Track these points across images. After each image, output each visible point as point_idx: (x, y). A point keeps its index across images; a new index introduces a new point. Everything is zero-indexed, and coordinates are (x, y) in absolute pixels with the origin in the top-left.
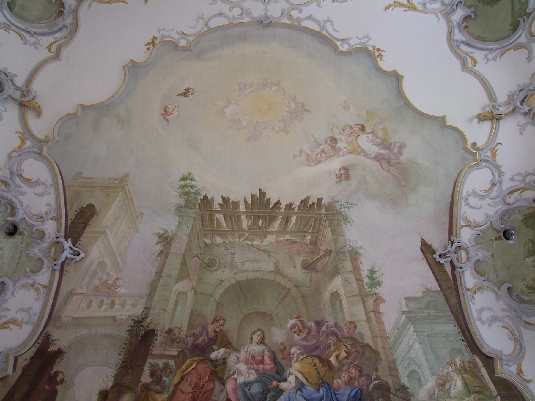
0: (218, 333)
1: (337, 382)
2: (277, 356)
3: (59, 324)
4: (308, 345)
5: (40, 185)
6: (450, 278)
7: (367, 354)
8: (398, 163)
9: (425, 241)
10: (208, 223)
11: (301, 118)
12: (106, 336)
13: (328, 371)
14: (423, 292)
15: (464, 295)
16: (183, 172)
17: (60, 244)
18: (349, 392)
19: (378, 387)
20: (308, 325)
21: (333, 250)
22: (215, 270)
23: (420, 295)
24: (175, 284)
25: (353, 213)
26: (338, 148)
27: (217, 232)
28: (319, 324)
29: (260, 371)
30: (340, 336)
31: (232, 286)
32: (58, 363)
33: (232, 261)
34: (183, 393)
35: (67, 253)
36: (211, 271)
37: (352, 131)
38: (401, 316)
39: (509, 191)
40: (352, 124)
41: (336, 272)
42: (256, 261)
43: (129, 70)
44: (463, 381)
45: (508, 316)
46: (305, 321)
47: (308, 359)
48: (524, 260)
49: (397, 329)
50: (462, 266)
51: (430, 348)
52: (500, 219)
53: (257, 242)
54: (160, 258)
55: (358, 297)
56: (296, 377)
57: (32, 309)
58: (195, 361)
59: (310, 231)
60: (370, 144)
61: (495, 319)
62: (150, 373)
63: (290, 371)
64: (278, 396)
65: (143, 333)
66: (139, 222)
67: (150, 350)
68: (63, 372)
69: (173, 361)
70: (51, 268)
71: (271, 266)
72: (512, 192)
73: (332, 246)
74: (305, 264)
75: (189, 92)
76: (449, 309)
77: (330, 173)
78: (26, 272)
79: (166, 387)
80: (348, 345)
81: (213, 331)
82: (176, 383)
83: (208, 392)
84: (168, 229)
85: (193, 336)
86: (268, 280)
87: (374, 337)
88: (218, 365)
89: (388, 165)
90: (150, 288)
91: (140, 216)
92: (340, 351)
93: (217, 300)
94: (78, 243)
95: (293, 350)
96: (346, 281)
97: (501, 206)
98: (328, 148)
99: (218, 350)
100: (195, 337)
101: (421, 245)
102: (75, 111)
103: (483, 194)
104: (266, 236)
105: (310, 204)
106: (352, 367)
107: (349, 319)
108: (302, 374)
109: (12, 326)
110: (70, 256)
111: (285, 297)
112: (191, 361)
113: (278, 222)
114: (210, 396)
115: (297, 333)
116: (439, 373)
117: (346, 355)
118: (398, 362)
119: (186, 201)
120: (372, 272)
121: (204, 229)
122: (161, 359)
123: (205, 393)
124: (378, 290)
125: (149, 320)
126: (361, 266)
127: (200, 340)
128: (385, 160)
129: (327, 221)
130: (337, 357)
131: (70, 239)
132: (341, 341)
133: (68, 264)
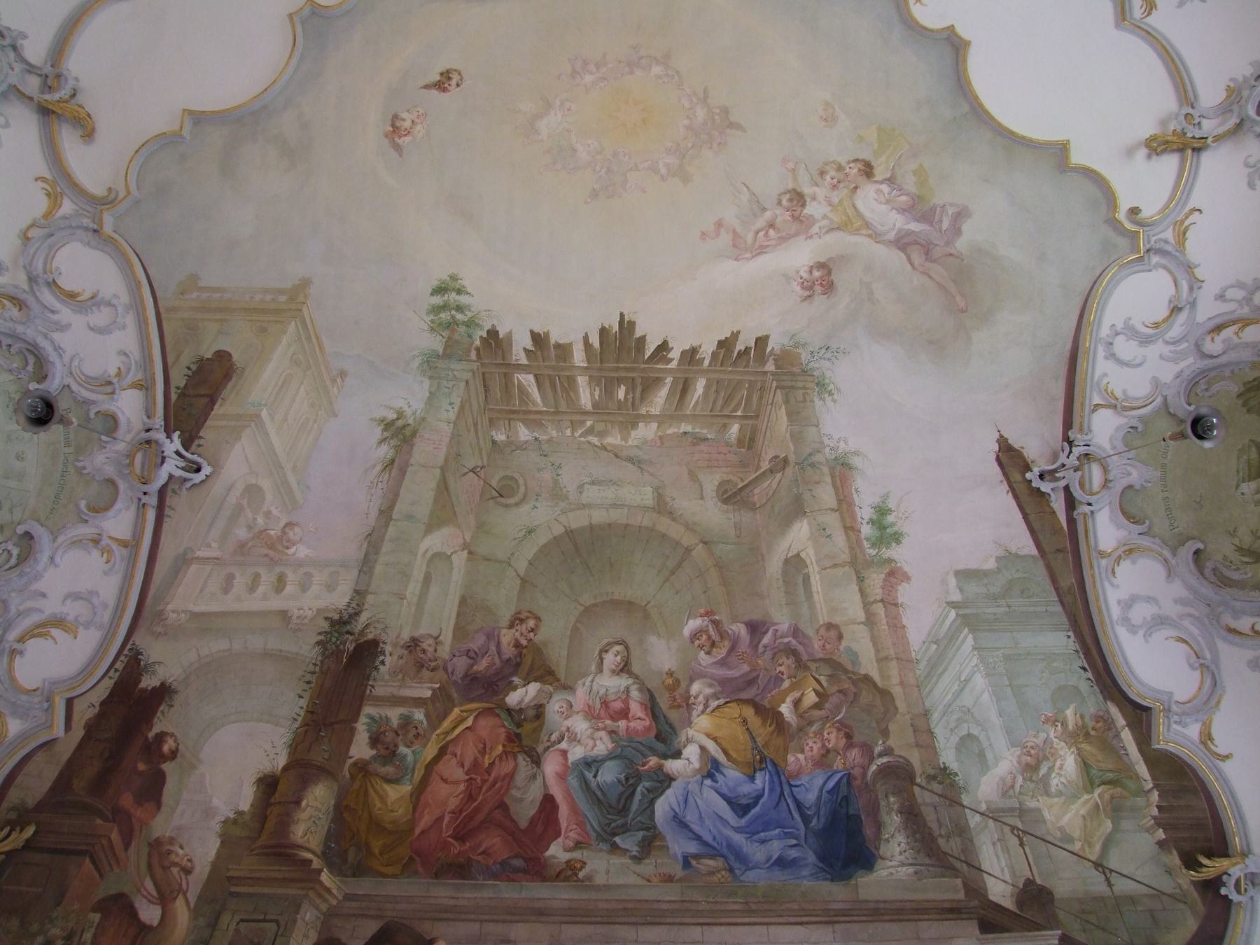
0: (523, 648)
1: (794, 760)
2: (658, 700)
3: (160, 629)
4: (730, 676)
5: (102, 308)
6: (1062, 528)
7: (866, 697)
8: (951, 255)
9: (1007, 439)
10: (499, 395)
11: (720, 143)
12: (266, 655)
13: (776, 734)
14: (998, 559)
15: (1092, 567)
16: (440, 274)
17: (153, 445)
18: (821, 782)
19: (885, 771)
20: (730, 632)
21: (792, 458)
22: (517, 504)
23: (991, 564)
24: (425, 536)
25: (840, 373)
26: (807, 219)
27: (521, 416)
28: (756, 628)
29: (621, 734)
30: (805, 657)
31: (557, 540)
32: (163, 712)
33: (556, 482)
34: (445, 781)
35: (172, 467)
36: (506, 506)
37: (840, 176)
38: (945, 612)
39: (1211, 324)
41: (797, 509)
42: (612, 482)
43: (303, 23)
44: (1080, 759)
45: (1190, 615)
46: (725, 621)
47: (729, 707)
48: (1237, 486)
49: (935, 643)
50: (1092, 499)
51: (1010, 685)
52: (1185, 391)
53: (614, 440)
54: (387, 475)
55: (847, 568)
56: (703, 748)
57: (97, 593)
58: (471, 711)
59: (739, 413)
60: (884, 208)
61: (1160, 621)
62: (370, 738)
63: (687, 734)
64: (661, 790)
65: (351, 648)
66: (336, 392)
67: (369, 687)
68: (176, 734)
69: (422, 710)
70: (136, 501)
71: (647, 496)
72: (1219, 328)
73: (790, 450)
74: (726, 491)
75: (450, 79)
76: (1056, 599)
77: (787, 277)
78: (79, 511)
79: (407, 770)
80: (822, 677)
81: (512, 645)
82: (429, 759)
83: (503, 780)
84: (406, 408)
85: (467, 655)
86: (640, 527)
87: (882, 660)
88: (525, 720)
89: (926, 259)
90: (365, 546)
91: (339, 380)
92: (804, 691)
93: (522, 573)
94: (196, 442)
95: (695, 688)
96: (821, 532)
97: (1191, 360)
98: (783, 216)
99: (524, 686)
100: (469, 657)
101: (997, 449)
102: (176, 128)
103: (1150, 331)
104: (634, 425)
105: (740, 350)
106: (829, 727)
107: (826, 618)
108: (716, 741)
109: (55, 632)
110: (179, 473)
111: (679, 565)
112: (462, 711)
113: (663, 392)
114: (508, 790)
115: (706, 649)
116: (1028, 742)
117: (817, 700)
118: (935, 716)
119: (446, 342)
120: (882, 511)
121: (489, 409)
122: (394, 706)
123: (494, 785)
124: (894, 552)
125: (365, 619)
126: (855, 496)
127: (482, 665)
128: (919, 247)
129: (779, 391)
130: (797, 703)
131: (177, 433)
132: (806, 668)
133: (174, 491)
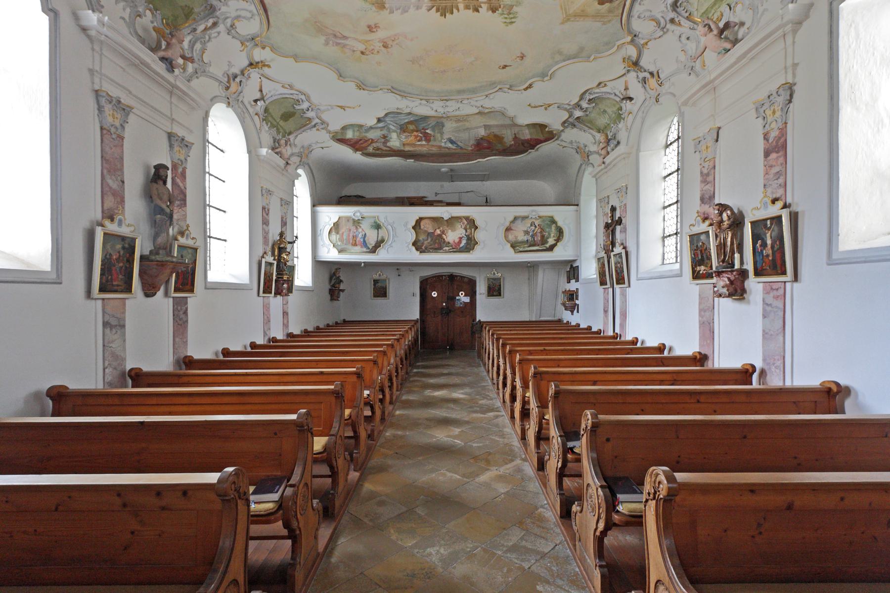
40: (372, 55)
